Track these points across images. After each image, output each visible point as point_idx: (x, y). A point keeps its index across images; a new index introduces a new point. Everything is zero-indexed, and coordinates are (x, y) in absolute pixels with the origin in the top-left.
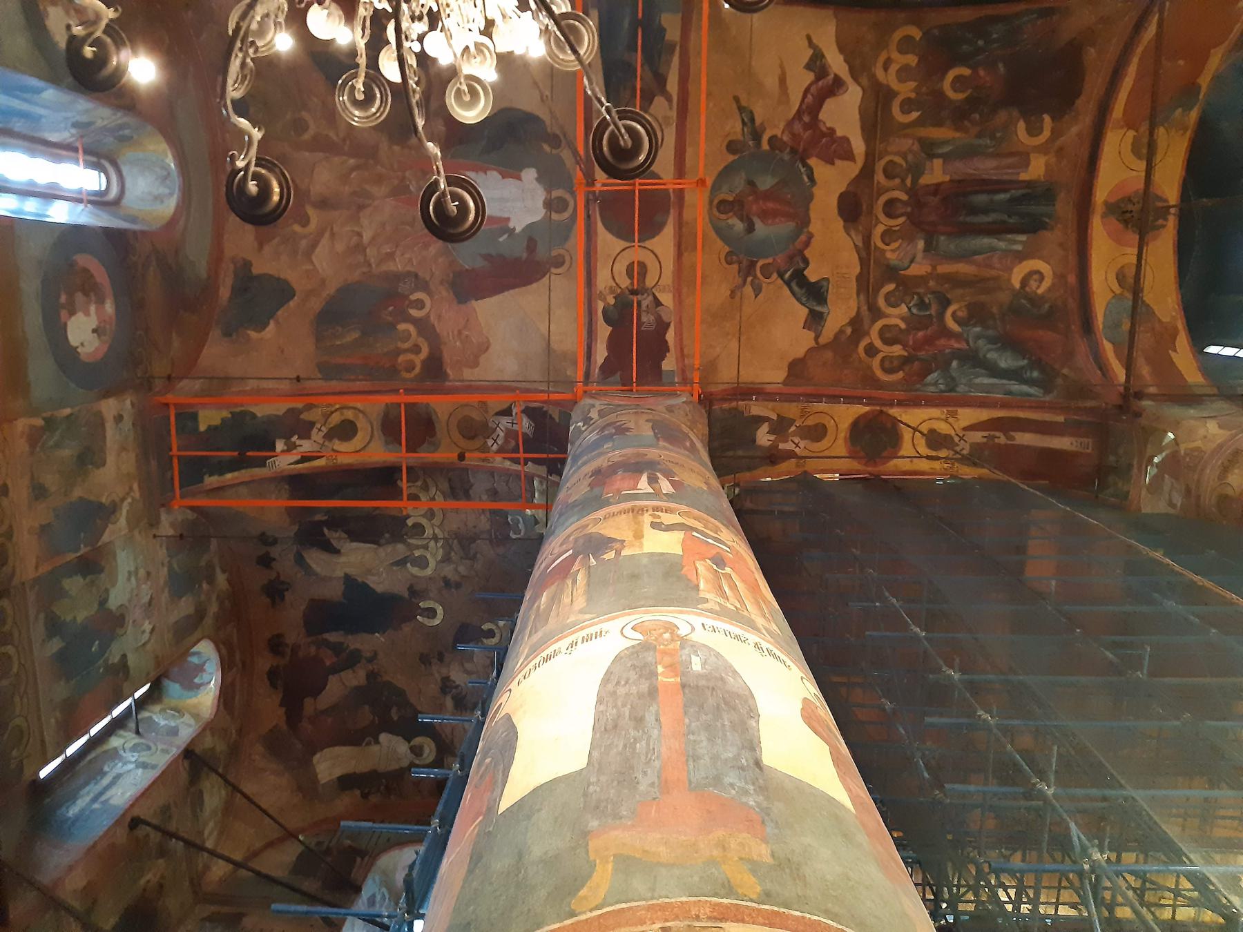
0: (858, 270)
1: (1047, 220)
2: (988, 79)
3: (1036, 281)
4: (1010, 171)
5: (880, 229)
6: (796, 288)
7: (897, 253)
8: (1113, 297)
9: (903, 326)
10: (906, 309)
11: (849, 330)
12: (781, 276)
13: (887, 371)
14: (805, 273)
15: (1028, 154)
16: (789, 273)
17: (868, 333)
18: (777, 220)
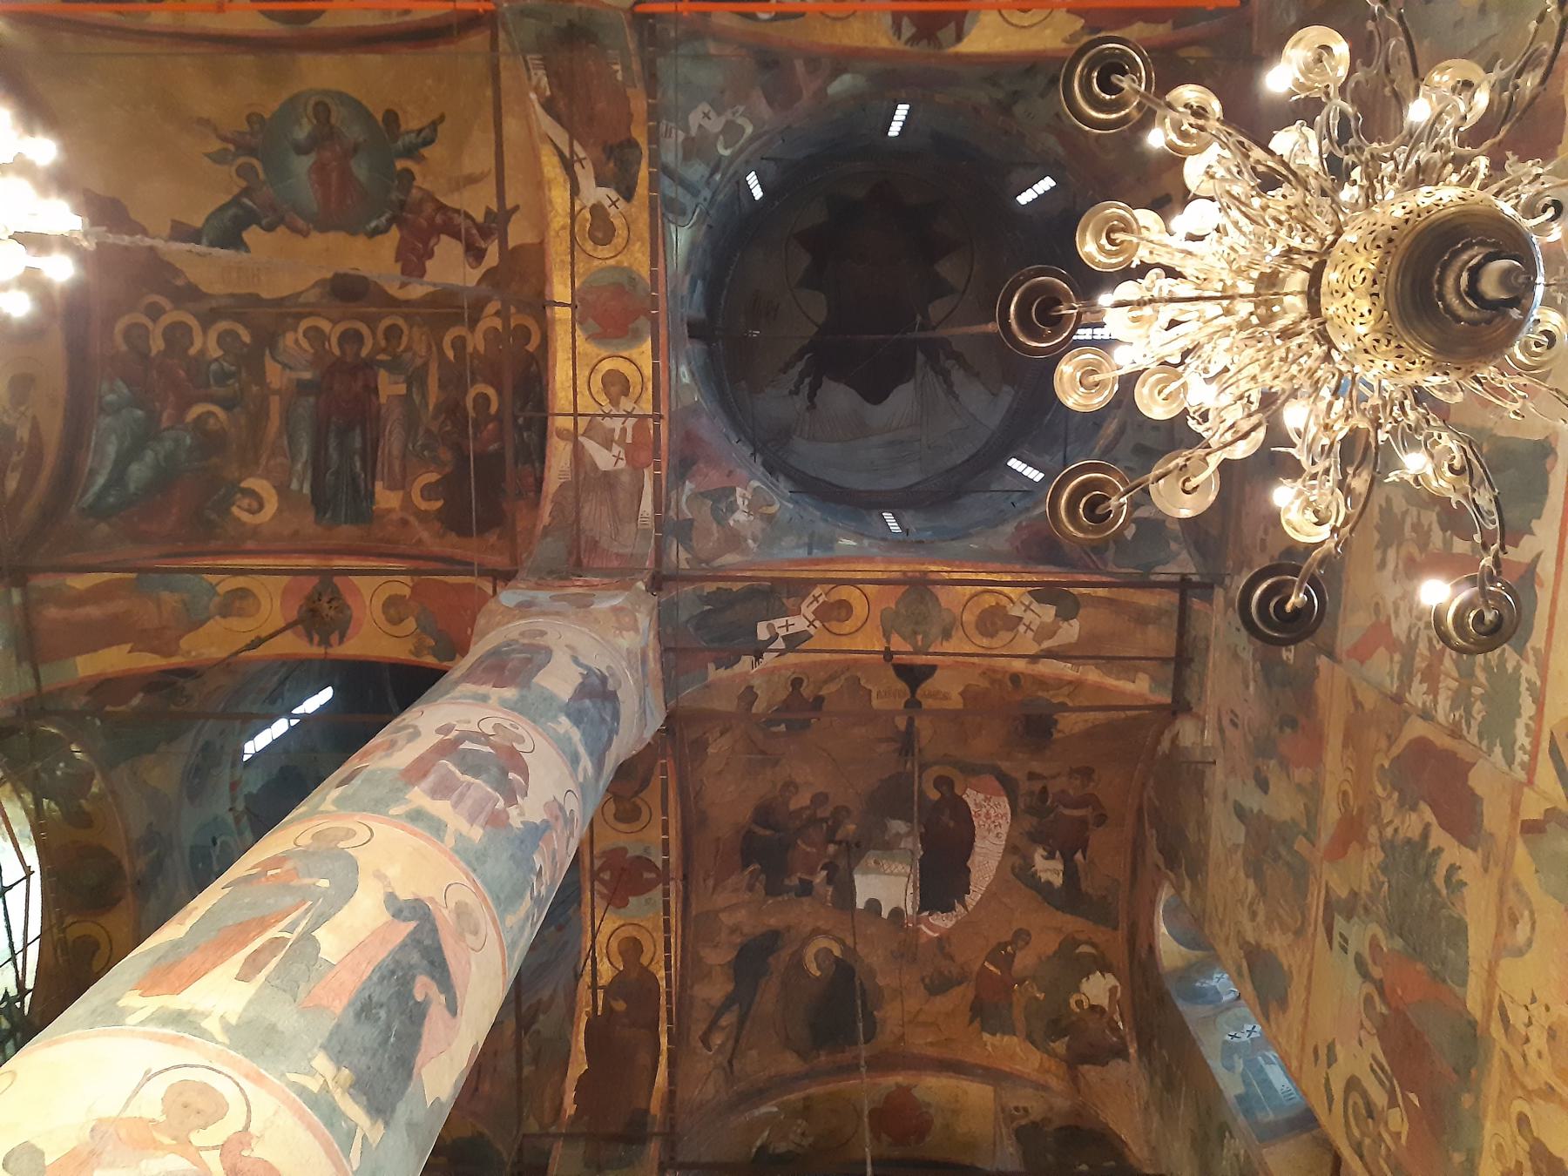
0: (265, 295)
1: (328, 516)
2: (485, 432)
3: (249, 505)
4: (386, 470)
5: (325, 326)
6: (232, 212)
7: (295, 346)
8: (211, 584)
9: (192, 351)
10: (215, 356)
11: (179, 282)
12: (246, 192)
13: (127, 334)
14: (254, 226)
15: (403, 488)
16: (250, 203)
17: (176, 308)
18: (316, 186)
